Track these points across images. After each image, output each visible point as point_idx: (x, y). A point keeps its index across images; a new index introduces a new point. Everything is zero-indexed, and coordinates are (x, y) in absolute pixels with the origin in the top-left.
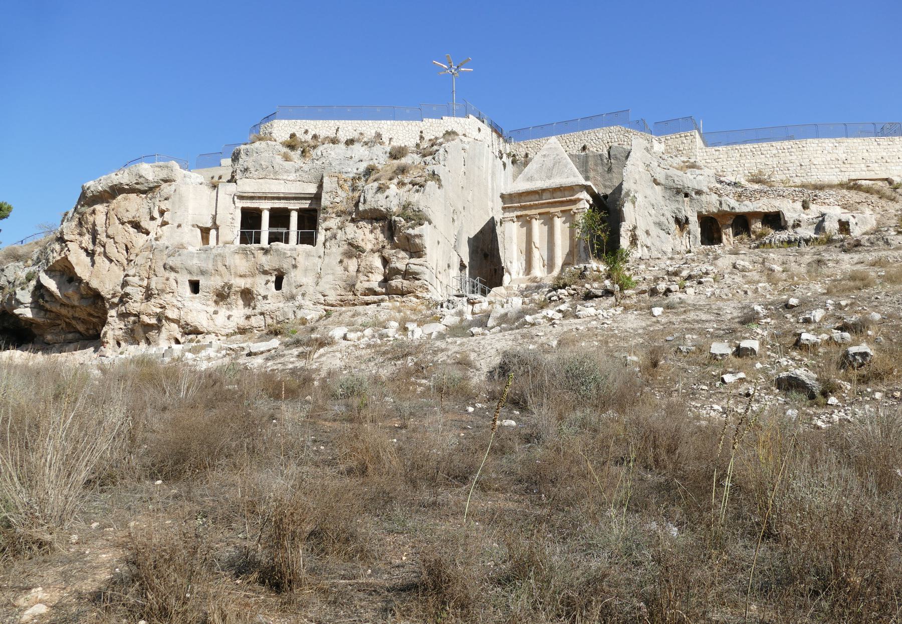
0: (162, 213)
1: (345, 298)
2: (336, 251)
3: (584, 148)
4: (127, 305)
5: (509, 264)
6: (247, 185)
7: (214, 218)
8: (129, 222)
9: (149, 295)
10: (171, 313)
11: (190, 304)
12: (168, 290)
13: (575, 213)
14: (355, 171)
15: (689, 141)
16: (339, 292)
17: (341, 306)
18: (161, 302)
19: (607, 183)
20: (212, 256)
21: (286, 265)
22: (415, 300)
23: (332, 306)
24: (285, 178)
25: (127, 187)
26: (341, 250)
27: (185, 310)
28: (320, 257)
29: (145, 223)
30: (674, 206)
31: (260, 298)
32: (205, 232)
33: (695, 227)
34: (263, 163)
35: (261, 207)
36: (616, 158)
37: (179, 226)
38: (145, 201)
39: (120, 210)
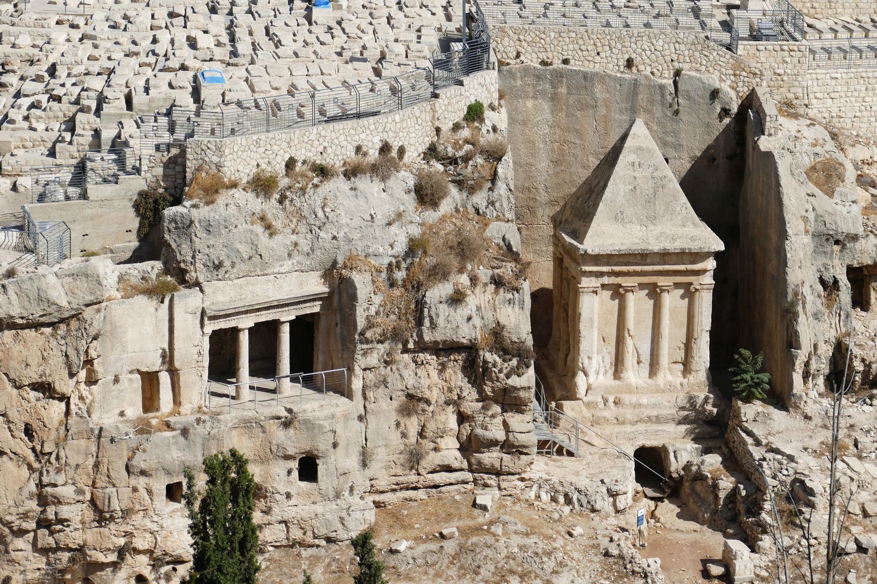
0: (89, 362)
1: (401, 479)
2: (386, 408)
3: (630, 63)
4: (60, 536)
5: (586, 361)
6: (221, 294)
7: (168, 357)
8: (29, 385)
9: (102, 516)
10: (141, 543)
11: (170, 521)
12: (138, 507)
13: (697, 290)
14: (390, 252)
15: (795, 60)
16: (393, 472)
17: (393, 490)
18: (129, 528)
19: (670, 139)
20: (199, 441)
21: (322, 445)
22: (521, 484)
23: (383, 492)
24: (276, 270)
25: (20, 321)
26: (395, 404)
27: (164, 533)
28: (361, 418)
29: (64, 385)
30: (821, 261)
31: (277, 496)
32: (150, 380)
33: (845, 294)
34: (239, 246)
35: (241, 326)
36: (689, 97)
37: (116, 380)
38: (54, 343)
39: (13, 364)
